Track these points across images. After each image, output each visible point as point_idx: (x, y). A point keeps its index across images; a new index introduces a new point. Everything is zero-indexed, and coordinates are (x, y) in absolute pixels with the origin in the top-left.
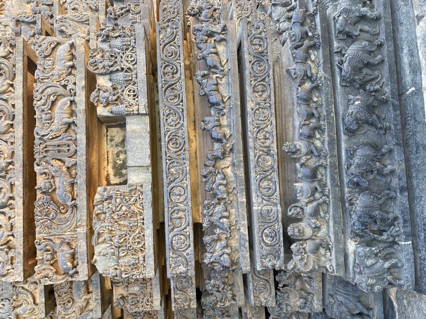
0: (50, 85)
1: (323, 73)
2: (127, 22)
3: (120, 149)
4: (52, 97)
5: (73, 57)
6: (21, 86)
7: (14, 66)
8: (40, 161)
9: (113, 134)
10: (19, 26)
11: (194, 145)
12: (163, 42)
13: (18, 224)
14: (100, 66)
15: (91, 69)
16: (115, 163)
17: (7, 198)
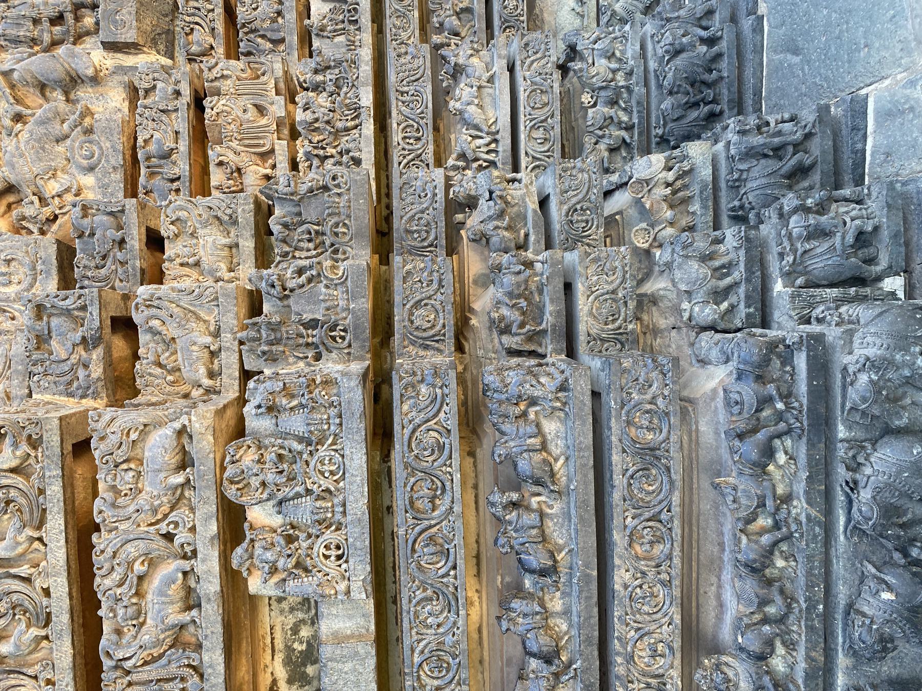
0: (132, 537)
1: (805, 505)
2: (315, 303)
3: (301, 615)
5: (185, 462)
6: (63, 542)
7: (42, 492)
10: (45, 318)
11: (475, 612)
12: (410, 422)
14: (255, 482)
15: (231, 492)
16: (289, 649)
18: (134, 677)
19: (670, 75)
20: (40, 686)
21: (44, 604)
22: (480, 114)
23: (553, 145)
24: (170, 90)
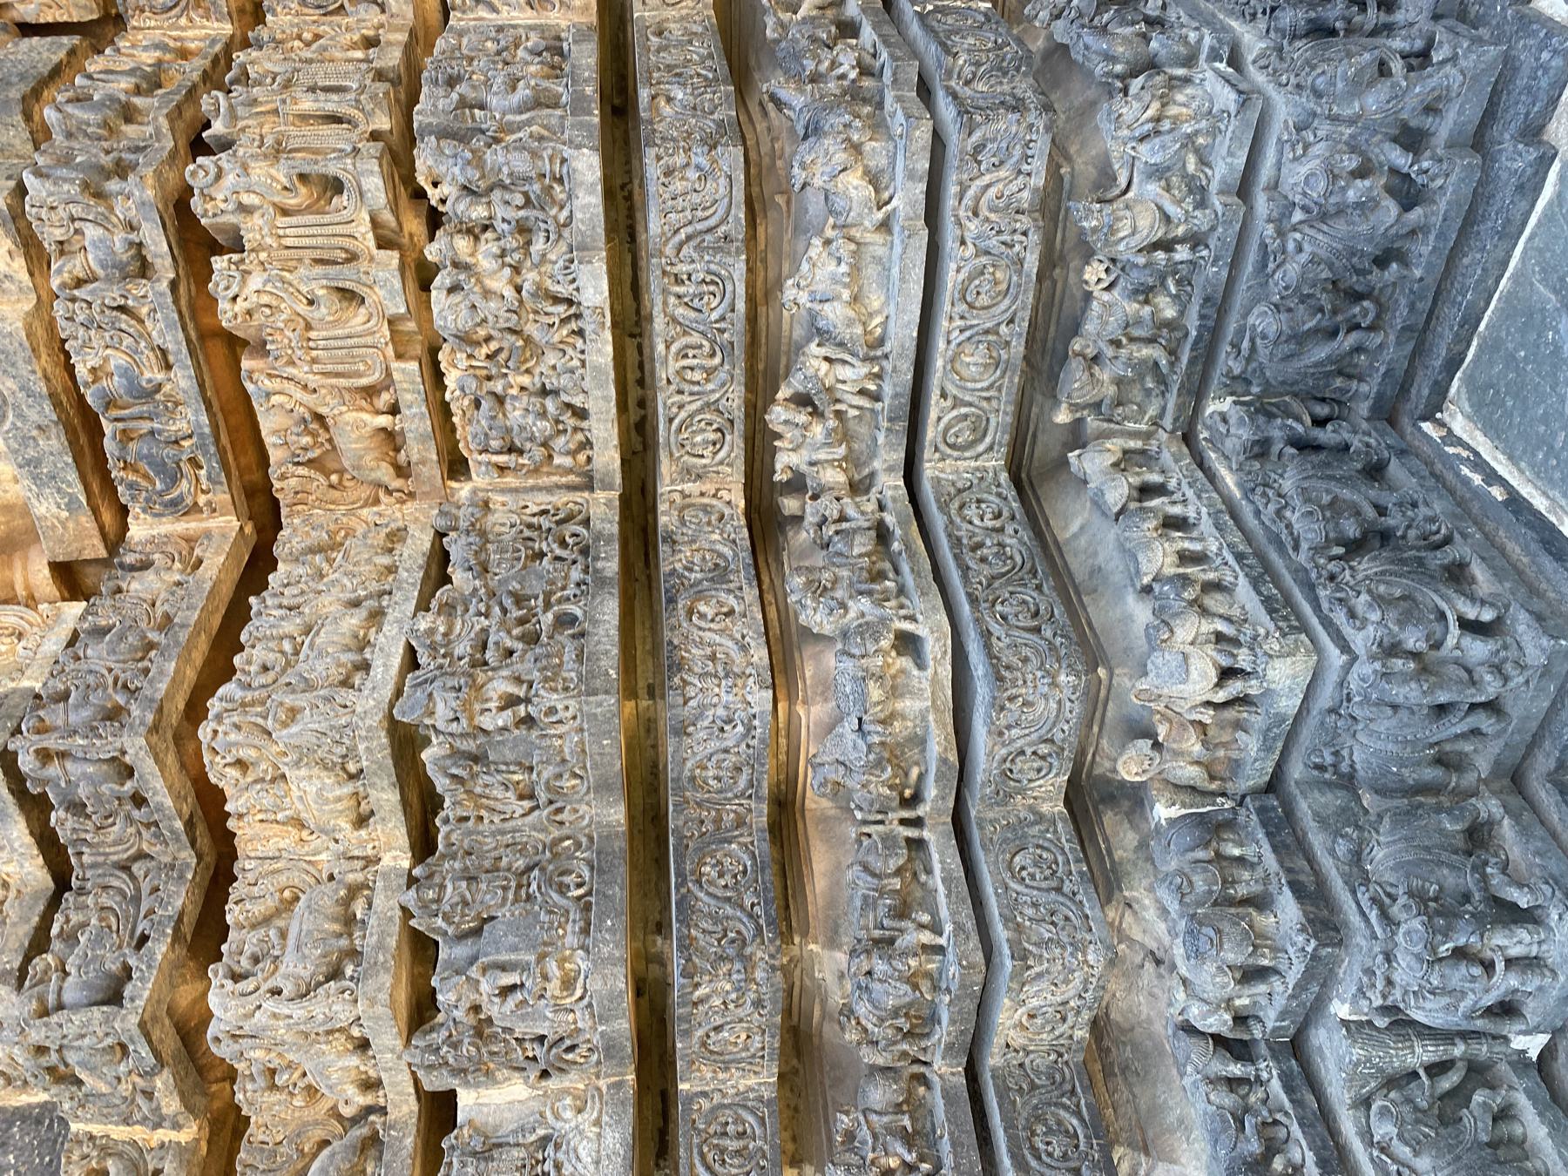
19: (1293, 269)
22: (850, 323)
23: (1002, 377)
24: (119, 239)
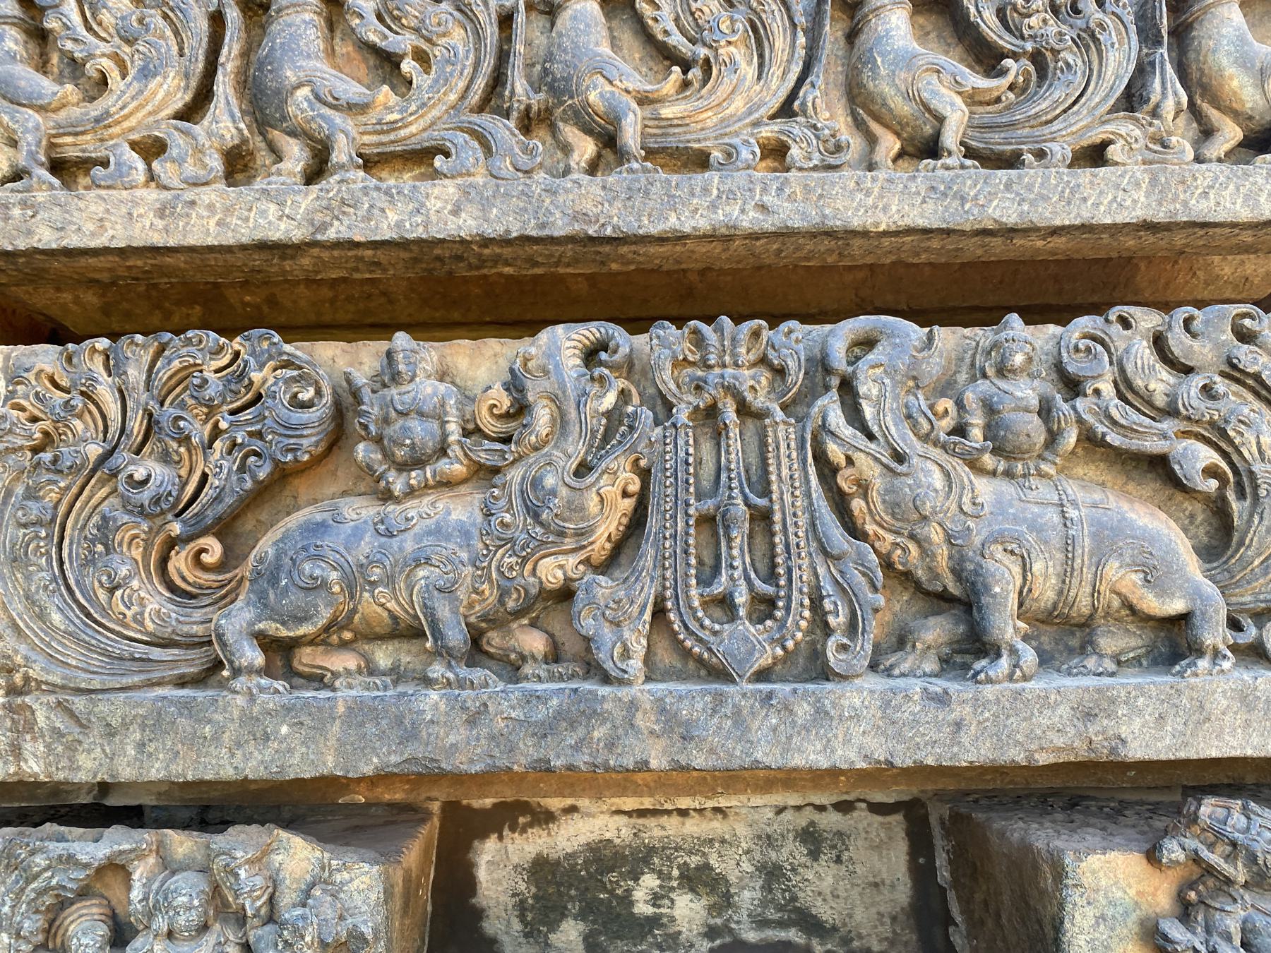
3: (748, 898)
4: (1207, 456)
8: (629, 367)
9: (857, 850)
13: (98, 209)
17: (320, 127)
18: (783, 432)
20: (756, 124)
21: (1055, 147)
